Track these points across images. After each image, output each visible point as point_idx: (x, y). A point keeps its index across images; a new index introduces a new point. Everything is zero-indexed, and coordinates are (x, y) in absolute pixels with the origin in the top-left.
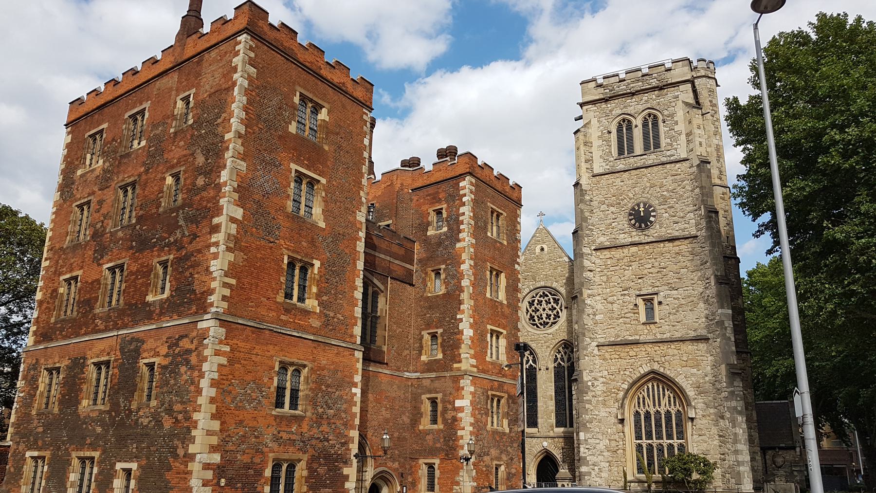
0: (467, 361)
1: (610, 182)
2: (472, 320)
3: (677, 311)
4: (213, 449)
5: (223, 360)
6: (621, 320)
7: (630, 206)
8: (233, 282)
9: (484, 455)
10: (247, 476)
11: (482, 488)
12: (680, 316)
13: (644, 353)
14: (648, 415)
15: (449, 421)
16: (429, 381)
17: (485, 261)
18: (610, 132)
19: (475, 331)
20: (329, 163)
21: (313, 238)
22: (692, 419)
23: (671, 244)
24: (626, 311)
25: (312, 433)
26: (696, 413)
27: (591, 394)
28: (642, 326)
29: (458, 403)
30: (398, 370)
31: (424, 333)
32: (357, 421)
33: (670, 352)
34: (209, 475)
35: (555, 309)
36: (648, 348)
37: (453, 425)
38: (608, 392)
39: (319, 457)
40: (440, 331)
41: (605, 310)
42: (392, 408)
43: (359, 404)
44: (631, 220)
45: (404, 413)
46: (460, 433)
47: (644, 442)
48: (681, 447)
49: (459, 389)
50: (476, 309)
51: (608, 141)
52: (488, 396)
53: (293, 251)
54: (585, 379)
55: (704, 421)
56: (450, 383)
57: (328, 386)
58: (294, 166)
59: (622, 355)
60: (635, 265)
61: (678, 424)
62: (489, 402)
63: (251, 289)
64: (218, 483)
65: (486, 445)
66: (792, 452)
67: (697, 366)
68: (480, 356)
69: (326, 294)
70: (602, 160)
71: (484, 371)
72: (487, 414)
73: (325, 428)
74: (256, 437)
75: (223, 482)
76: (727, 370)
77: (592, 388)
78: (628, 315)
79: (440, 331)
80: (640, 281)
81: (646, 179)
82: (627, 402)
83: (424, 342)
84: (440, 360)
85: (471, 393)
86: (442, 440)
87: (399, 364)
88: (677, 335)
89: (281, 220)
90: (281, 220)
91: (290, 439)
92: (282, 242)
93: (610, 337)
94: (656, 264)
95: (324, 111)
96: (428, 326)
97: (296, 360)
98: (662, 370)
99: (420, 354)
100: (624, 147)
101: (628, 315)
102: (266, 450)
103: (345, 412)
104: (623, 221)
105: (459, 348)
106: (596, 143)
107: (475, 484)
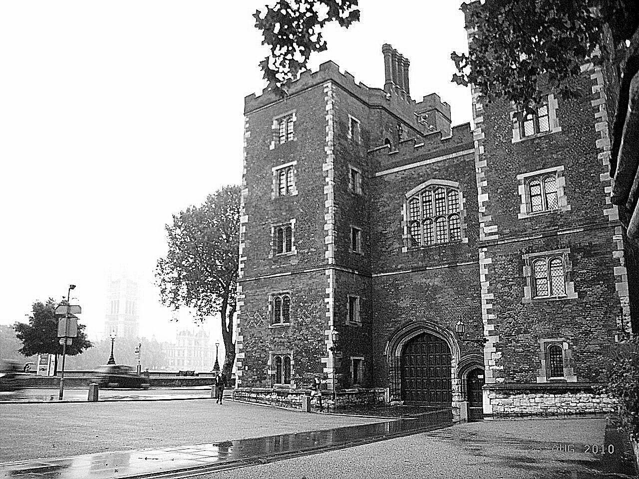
2: (485, 183)
4: (241, 351)
5: (242, 303)
8: (245, 258)
9: (518, 333)
10: (258, 365)
11: (515, 372)
20: (298, 148)
21: (289, 207)
25: (295, 336)
32: (331, 323)
34: (240, 364)
39: (301, 352)
43: (331, 310)
53: (276, 223)
57: (306, 302)
58: (274, 169)
63: (254, 258)
64: (245, 369)
69: (301, 239)
71: (514, 234)
73: (304, 331)
74: (262, 343)
75: (247, 368)
89: (269, 208)
90: (269, 208)
91: (281, 342)
92: (270, 220)
95: (294, 114)
97: (281, 292)
102: (267, 349)
103: (320, 318)
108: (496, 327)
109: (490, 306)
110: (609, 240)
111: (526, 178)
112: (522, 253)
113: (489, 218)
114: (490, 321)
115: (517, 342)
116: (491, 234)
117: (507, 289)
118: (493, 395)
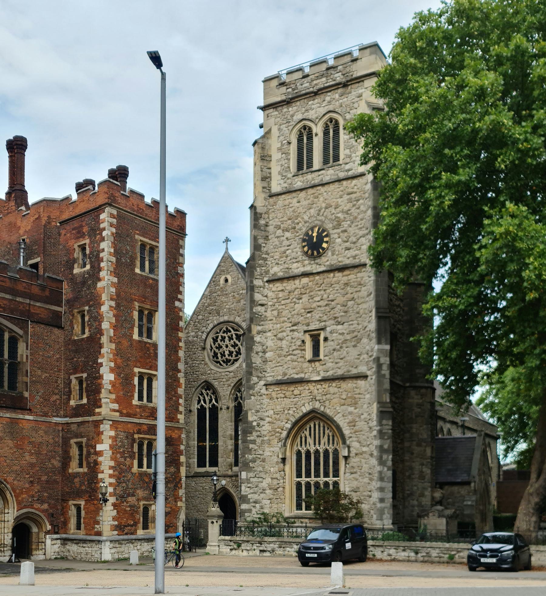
0: (108, 407)
1: (287, 202)
3: (341, 347)
6: (289, 358)
7: (304, 230)
9: (129, 495)
12: (344, 352)
13: (307, 392)
14: (308, 453)
15: (92, 465)
16: (76, 425)
17: (132, 300)
18: (289, 143)
19: (118, 375)
22: (346, 458)
23: (340, 274)
24: (294, 348)
26: (349, 452)
27: (254, 434)
28: (307, 364)
29: (99, 447)
30: (45, 415)
31: (72, 377)
33: (332, 390)
35: (217, 348)
36: (311, 386)
37: (94, 468)
38: (273, 432)
40: (85, 375)
41: (276, 347)
42: (38, 453)
44: (304, 247)
45: (54, 457)
46: (100, 476)
47: (304, 480)
48: (336, 484)
49: (100, 433)
50: (118, 353)
51: (287, 154)
52: (134, 440)
54: (250, 419)
55: (357, 459)
56: (92, 428)
59: (288, 394)
60: (305, 298)
61: (331, 463)
62: (136, 446)
65: (130, 486)
66: (466, 487)
67: (355, 404)
68: (123, 400)
70: (280, 177)
71: (129, 415)
72: (132, 457)
76: (378, 409)
77: (257, 428)
78: (295, 352)
79: (85, 375)
80: (309, 315)
81: (321, 199)
82: (289, 441)
83: (72, 386)
84: (85, 404)
85: (110, 437)
86: (86, 483)
87: (46, 409)
88: (340, 372)
93: (277, 376)
94: (325, 296)
96: (75, 372)
98: (322, 409)
99: (69, 399)
100: (303, 162)
101: (295, 352)
104: (297, 249)
105: (99, 392)
106: (276, 156)
107: (116, 523)
108: (115, 489)
109: (111, 472)
110: (180, 436)
111: (139, 372)
112: (134, 433)
113: (113, 396)
114: (111, 484)
115: (127, 503)
116: (115, 411)
117: (123, 460)
118: (112, 545)
